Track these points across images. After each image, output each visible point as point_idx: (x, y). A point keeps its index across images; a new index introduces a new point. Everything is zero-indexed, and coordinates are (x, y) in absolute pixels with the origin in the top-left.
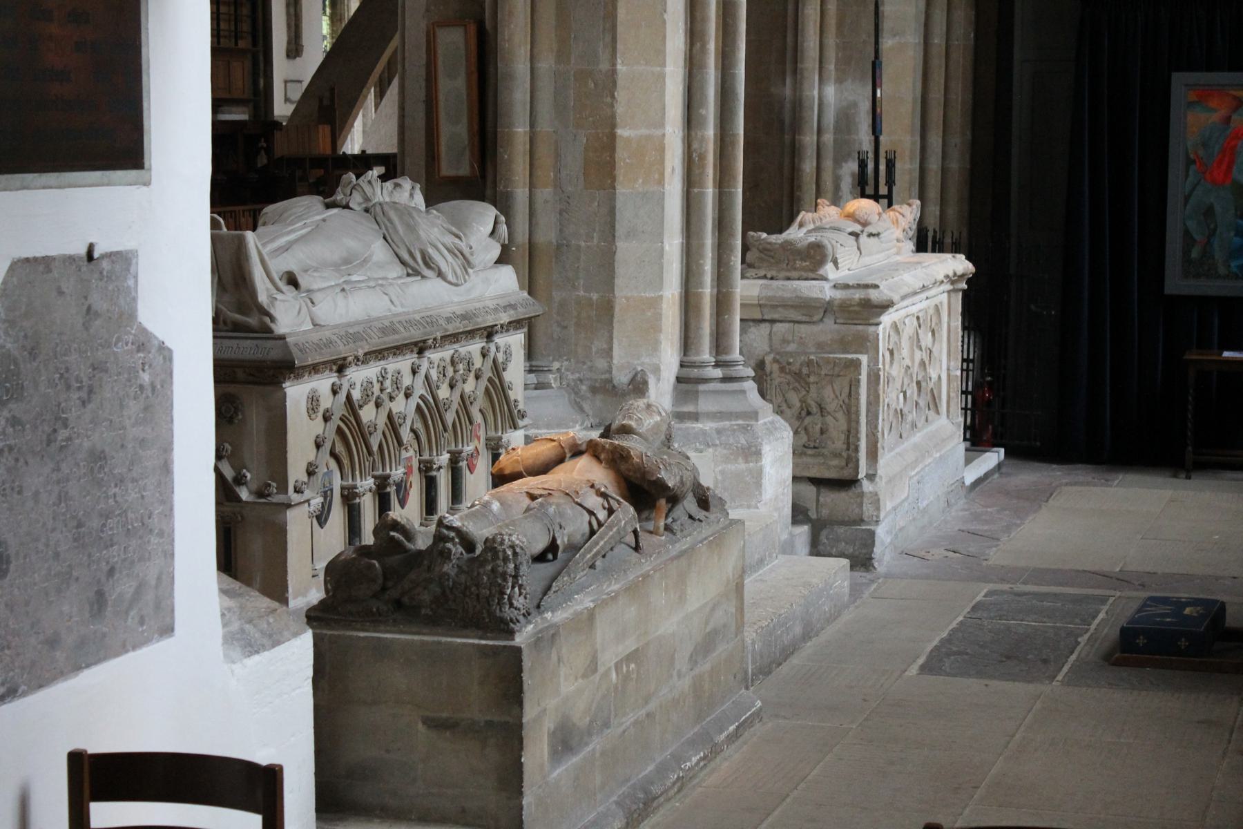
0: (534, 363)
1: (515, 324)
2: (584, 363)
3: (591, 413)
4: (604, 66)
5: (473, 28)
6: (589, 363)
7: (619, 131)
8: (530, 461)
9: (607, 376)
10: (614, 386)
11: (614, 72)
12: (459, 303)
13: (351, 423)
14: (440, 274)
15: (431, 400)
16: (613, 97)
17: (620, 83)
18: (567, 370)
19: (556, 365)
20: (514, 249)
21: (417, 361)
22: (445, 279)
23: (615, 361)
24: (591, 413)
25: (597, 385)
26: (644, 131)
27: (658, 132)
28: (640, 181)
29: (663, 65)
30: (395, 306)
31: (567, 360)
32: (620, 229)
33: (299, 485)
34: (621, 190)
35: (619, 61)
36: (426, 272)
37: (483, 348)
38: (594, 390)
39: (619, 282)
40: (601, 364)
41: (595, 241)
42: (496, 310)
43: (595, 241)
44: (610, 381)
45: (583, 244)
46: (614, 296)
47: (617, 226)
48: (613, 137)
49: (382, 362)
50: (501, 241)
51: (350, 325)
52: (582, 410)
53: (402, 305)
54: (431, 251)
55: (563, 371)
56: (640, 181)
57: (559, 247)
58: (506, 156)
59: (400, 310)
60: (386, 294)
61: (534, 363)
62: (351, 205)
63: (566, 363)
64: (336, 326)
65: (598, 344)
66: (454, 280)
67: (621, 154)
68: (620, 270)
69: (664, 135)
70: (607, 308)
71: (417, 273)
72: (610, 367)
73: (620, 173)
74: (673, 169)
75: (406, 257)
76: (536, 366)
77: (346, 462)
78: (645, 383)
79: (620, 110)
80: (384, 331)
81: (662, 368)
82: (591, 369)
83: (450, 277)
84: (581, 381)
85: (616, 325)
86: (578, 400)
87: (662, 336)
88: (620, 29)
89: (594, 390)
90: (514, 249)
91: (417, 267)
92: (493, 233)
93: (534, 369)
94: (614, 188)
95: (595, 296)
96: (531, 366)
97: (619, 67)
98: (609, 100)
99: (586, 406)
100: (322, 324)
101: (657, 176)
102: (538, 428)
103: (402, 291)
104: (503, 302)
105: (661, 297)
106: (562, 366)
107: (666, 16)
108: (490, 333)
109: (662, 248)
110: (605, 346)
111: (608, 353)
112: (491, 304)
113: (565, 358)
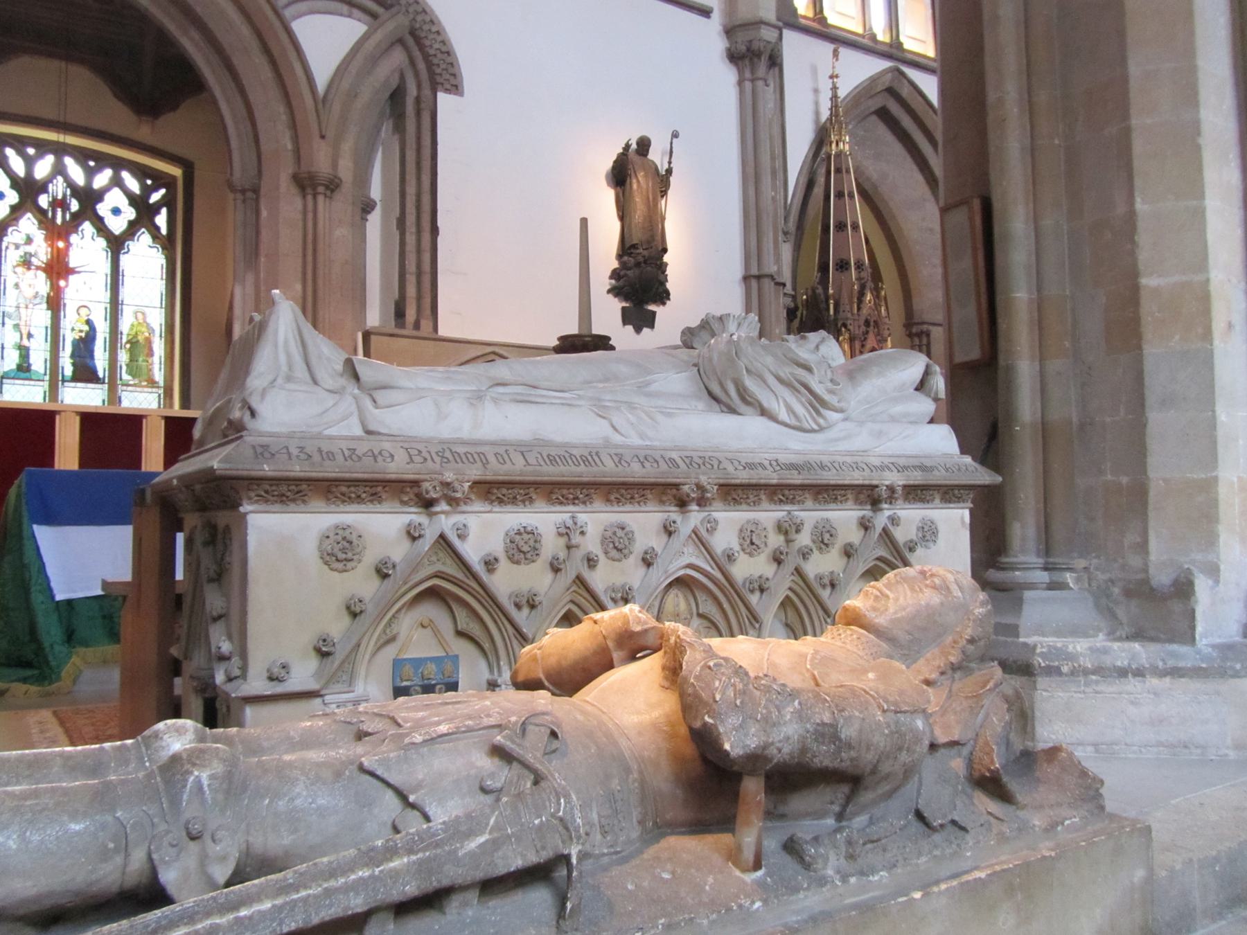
0: (1051, 560)
1: (949, 493)
2: (1115, 560)
3: (1125, 620)
4: (1121, 210)
5: (977, 204)
6: (1121, 561)
7: (1144, 281)
8: (552, 661)
9: (1141, 576)
10: (1152, 589)
11: (1131, 216)
12: (797, 453)
13: (474, 589)
14: (764, 412)
15: (718, 575)
16: (1133, 242)
17: (1141, 225)
18: (1097, 569)
19: (1081, 563)
20: (1018, 428)
21: (674, 516)
22: (773, 418)
23: (1153, 557)
24: (1125, 620)
25: (1131, 586)
26: (1176, 278)
27: (1198, 278)
28: (1177, 337)
29: (1201, 196)
30: (622, 435)
31: (1095, 557)
32: (1151, 398)
33: (276, 670)
34: (1148, 350)
35: (1138, 200)
36: (742, 407)
37: (863, 518)
38: (1128, 593)
39: (1152, 461)
40: (1135, 561)
41: (1122, 413)
42: (883, 468)
43: (1122, 413)
44: (1146, 581)
45: (1108, 420)
46: (1148, 478)
47: (1147, 393)
48: (1135, 289)
49: (571, 508)
50: (932, 395)
51: (464, 443)
52: (1113, 615)
53: (642, 436)
54: (750, 383)
55: (1092, 570)
56: (1177, 337)
57: (1082, 427)
58: (1005, 326)
59: (636, 441)
60: (604, 418)
61: (1051, 560)
62: (694, 346)
63: (1095, 561)
64: (428, 441)
65: (1131, 538)
66: (793, 422)
67: (1148, 309)
68: (1153, 444)
69: (1208, 280)
70: (1138, 496)
71: (732, 411)
72: (1146, 565)
73: (1148, 331)
74: (1230, 326)
75: (716, 390)
76: (1052, 563)
77: (487, 646)
78: (1190, 584)
79: (1144, 256)
80: (552, 460)
81: (1222, 567)
82: (1123, 567)
83: (783, 415)
84: (1112, 581)
85: (1152, 514)
86: (1111, 605)
87: (1221, 528)
88: (1137, 164)
89: (1128, 593)
90: (1018, 428)
91: (731, 403)
92: (921, 386)
93: (1050, 566)
94: (1140, 348)
95: (1125, 480)
96: (1046, 563)
97: (1139, 205)
98: (1129, 246)
99: (1121, 613)
100: (383, 431)
101: (1200, 330)
102: (1044, 635)
103: (651, 418)
104: (916, 462)
105: (1216, 479)
106: (1090, 564)
107: (1201, 141)
108: (870, 496)
109: (1214, 417)
110: (1139, 540)
111: (1143, 547)
112: (876, 461)
113: (1094, 555)
